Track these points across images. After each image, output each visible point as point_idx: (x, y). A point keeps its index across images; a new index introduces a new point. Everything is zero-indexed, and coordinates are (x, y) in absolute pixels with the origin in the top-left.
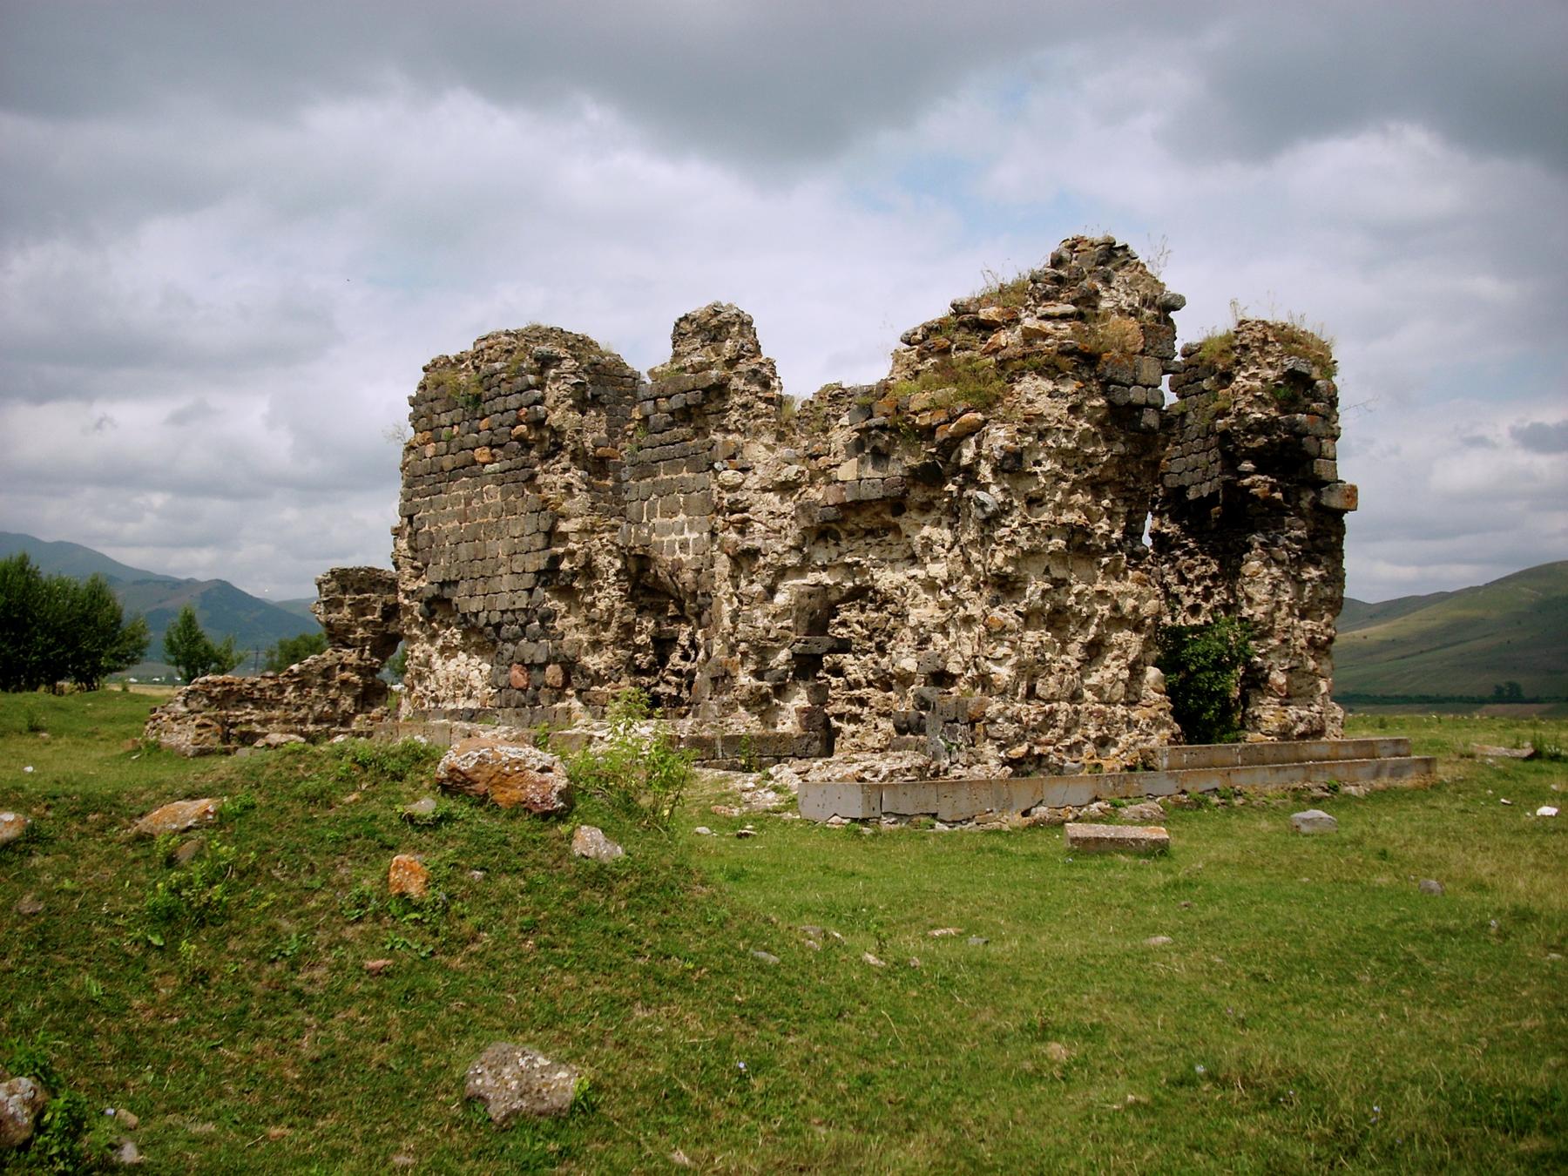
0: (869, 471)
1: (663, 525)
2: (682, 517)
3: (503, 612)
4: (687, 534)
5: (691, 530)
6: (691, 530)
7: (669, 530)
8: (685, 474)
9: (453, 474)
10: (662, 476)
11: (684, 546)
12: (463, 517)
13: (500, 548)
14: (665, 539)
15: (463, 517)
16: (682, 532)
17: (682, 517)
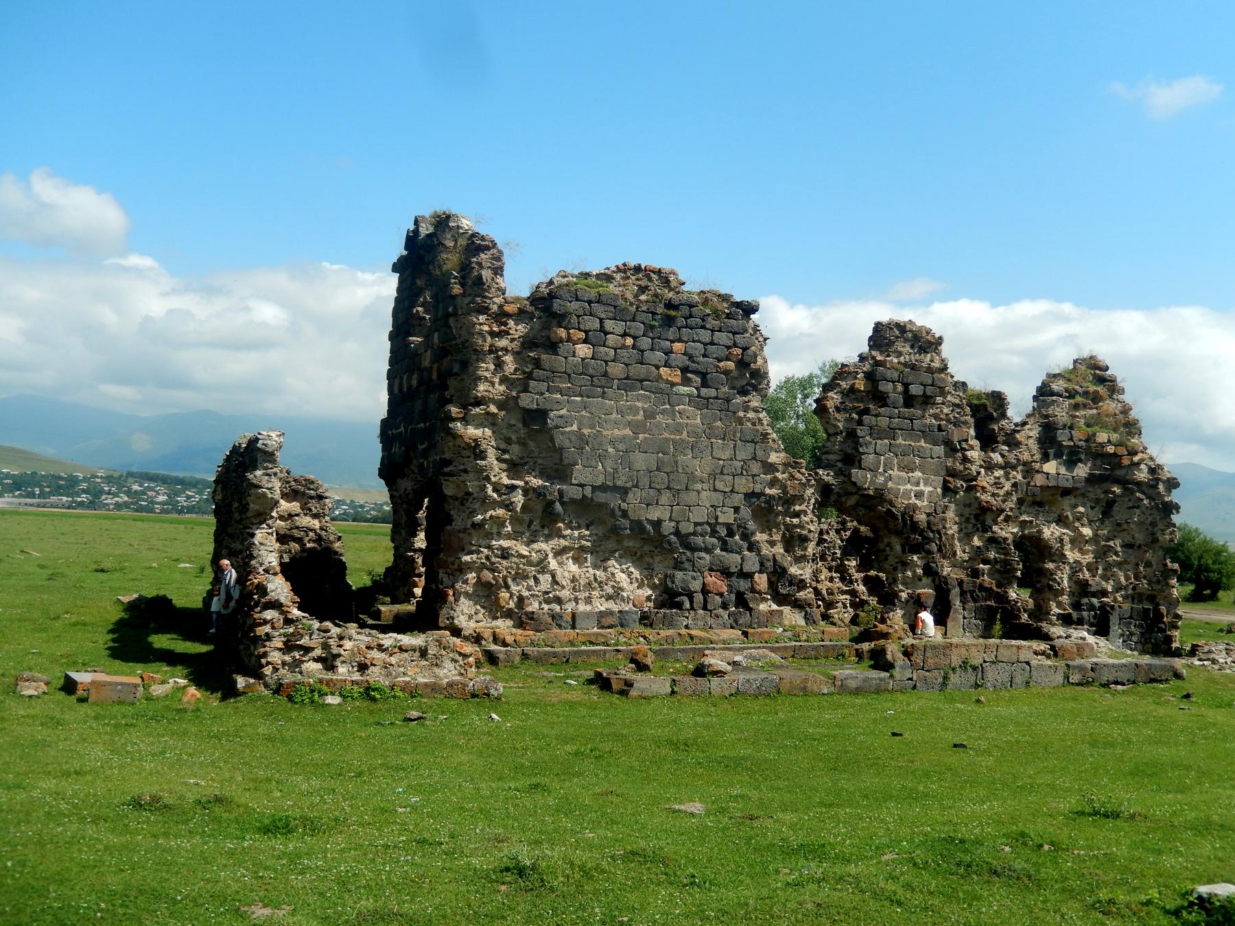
0: (1063, 470)
1: (899, 478)
2: (918, 474)
3: (696, 524)
4: (922, 487)
5: (925, 484)
6: (925, 484)
7: (901, 481)
8: (922, 443)
9: (630, 383)
10: (900, 441)
11: (919, 495)
12: (637, 428)
13: (700, 467)
14: (902, 488)
15: (637, 428)
16: (918, 484)
17: (918, 474)
